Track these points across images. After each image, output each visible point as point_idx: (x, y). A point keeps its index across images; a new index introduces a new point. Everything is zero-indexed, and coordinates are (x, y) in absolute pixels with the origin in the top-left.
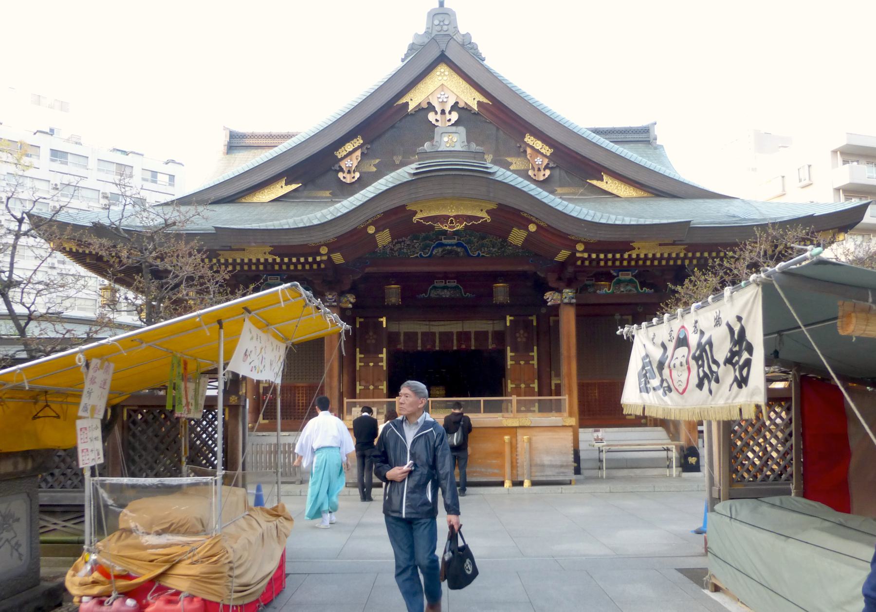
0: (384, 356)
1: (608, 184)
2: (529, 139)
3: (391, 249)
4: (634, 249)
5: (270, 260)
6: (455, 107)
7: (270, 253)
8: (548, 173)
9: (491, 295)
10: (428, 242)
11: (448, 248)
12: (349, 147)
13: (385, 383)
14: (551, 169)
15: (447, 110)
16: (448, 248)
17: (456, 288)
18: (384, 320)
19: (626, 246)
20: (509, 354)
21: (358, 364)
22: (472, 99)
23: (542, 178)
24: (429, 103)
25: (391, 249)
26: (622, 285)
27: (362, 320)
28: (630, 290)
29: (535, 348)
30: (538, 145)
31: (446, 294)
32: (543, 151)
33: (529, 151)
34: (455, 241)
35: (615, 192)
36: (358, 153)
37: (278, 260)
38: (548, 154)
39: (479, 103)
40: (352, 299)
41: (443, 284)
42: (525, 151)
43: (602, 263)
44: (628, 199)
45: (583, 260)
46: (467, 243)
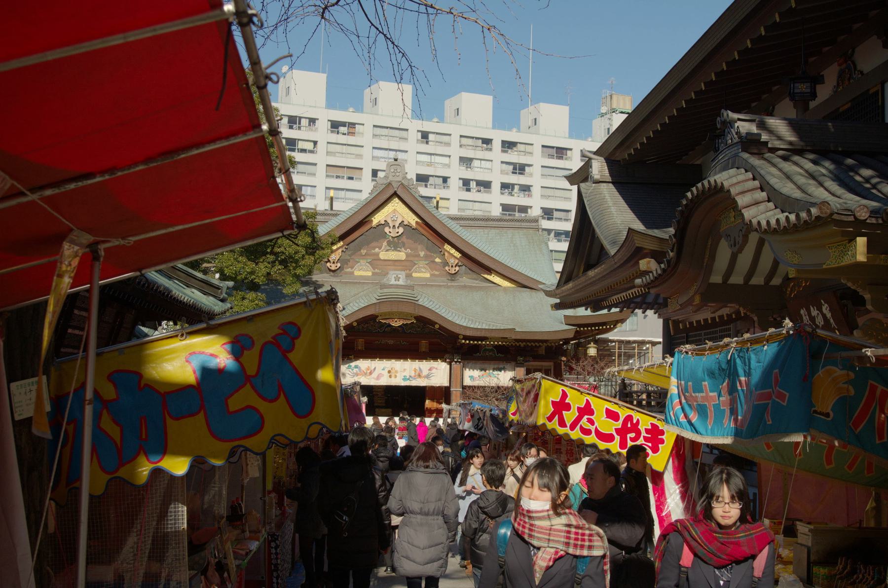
2: (447, 247)
8: (457, 268)
15: (397, 225)
30: (453, 251)
33: (446, 254)
36: (340, 251)
39: (417, 222)
44: (506, 289)
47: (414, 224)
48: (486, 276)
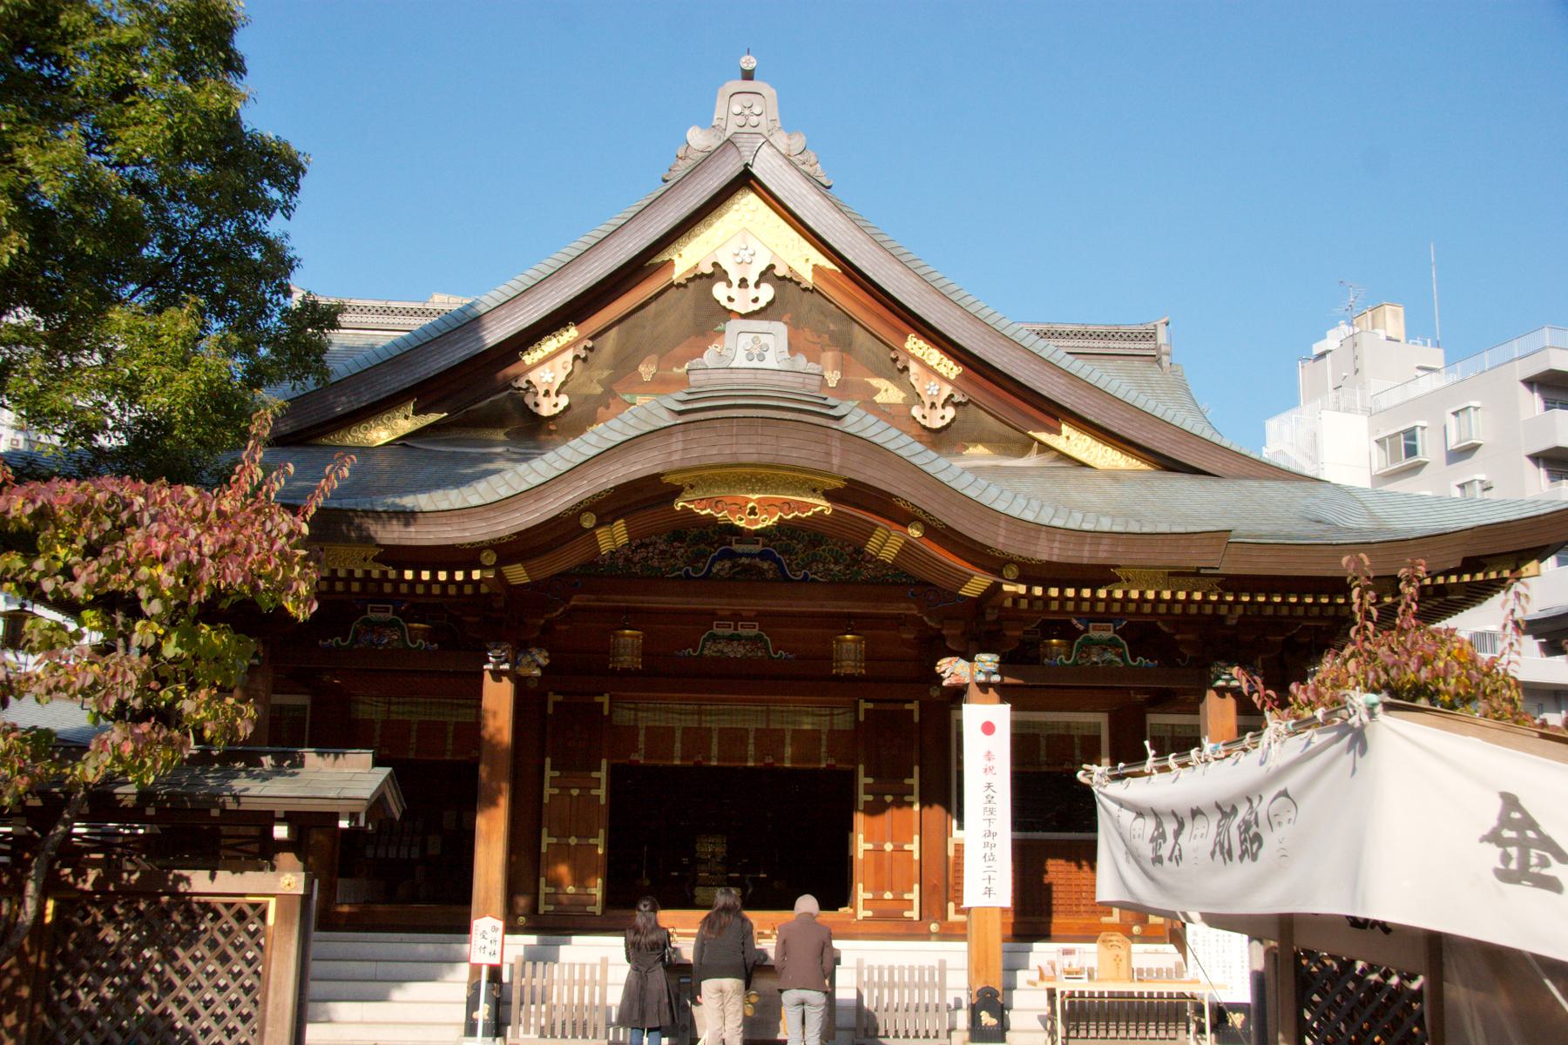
0: (602, 775)
1: (1071, 441)
2: (915, 345)
3: (627, 560)
4: (1119, 580)
5: (376, 574)
6: (767, 275)
7: (375, 559)
9: (828, 658)
10: (702, 546)
11: (744, 560)
12: (550, 345)
13: (602, 832)
14: (956, 405)
15: (752, 278)
16: (744, 560)
17: (758, 638)
18: (605, 699)
19: (1101, 575)
20: (863, 780)
21: (548, 791)
22: (803, 261)
23: (938, 424)
24: (715, 265)
25: (627, 560)
26: (1094, 650)
27: (560, 698)
28: (1111, 661)
29: (916, 769)
30: (934, 356)
31: (736, 651)
32: (942, 370)
33: (914, 367)
34: (758, 548)
35: (1083, 457)
37: (392, 574)
38: (952, 377)
39: (817, 269)
40: (542, 659)
41: (730, 631)
42: (906, 369)
43: (1055, 606)
45: (1016, 597)
46: (782, 553)
47: (808, 277)
48: (1043, 436)
